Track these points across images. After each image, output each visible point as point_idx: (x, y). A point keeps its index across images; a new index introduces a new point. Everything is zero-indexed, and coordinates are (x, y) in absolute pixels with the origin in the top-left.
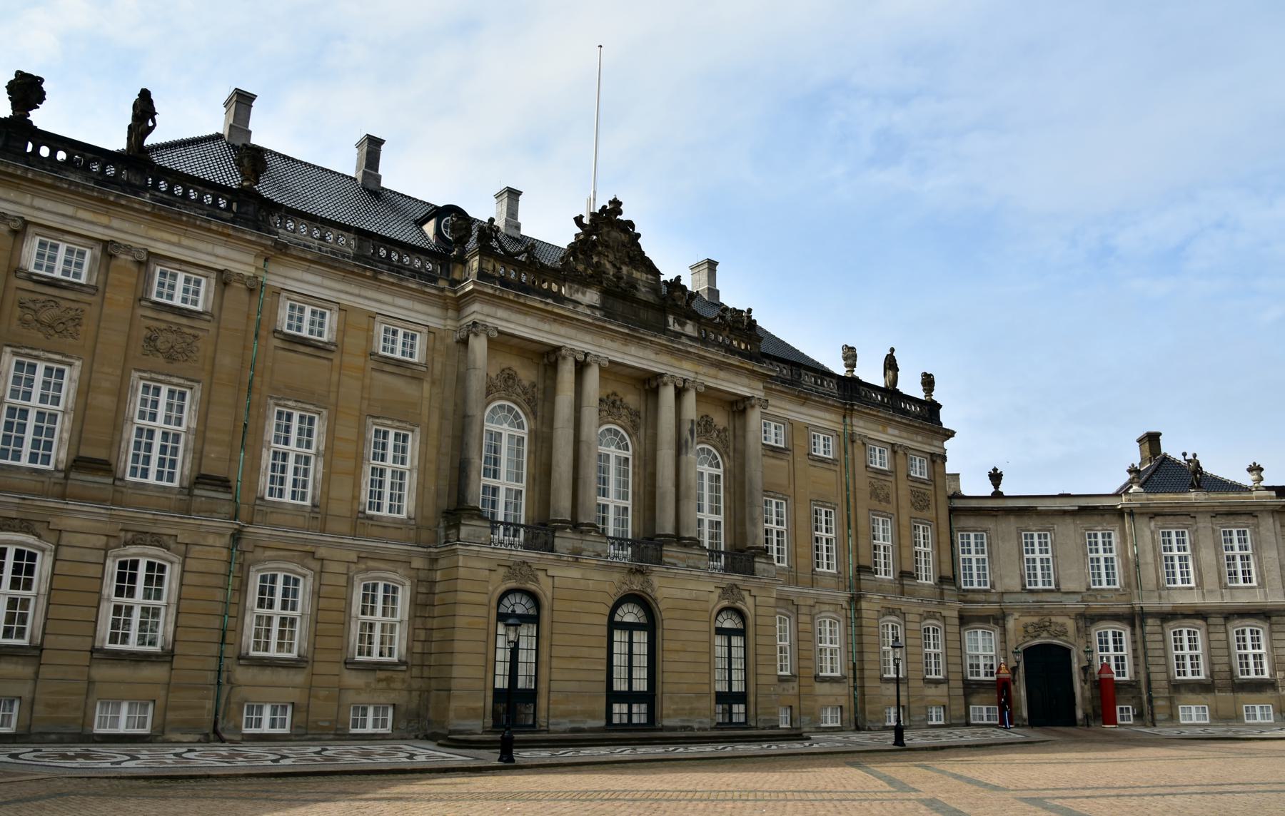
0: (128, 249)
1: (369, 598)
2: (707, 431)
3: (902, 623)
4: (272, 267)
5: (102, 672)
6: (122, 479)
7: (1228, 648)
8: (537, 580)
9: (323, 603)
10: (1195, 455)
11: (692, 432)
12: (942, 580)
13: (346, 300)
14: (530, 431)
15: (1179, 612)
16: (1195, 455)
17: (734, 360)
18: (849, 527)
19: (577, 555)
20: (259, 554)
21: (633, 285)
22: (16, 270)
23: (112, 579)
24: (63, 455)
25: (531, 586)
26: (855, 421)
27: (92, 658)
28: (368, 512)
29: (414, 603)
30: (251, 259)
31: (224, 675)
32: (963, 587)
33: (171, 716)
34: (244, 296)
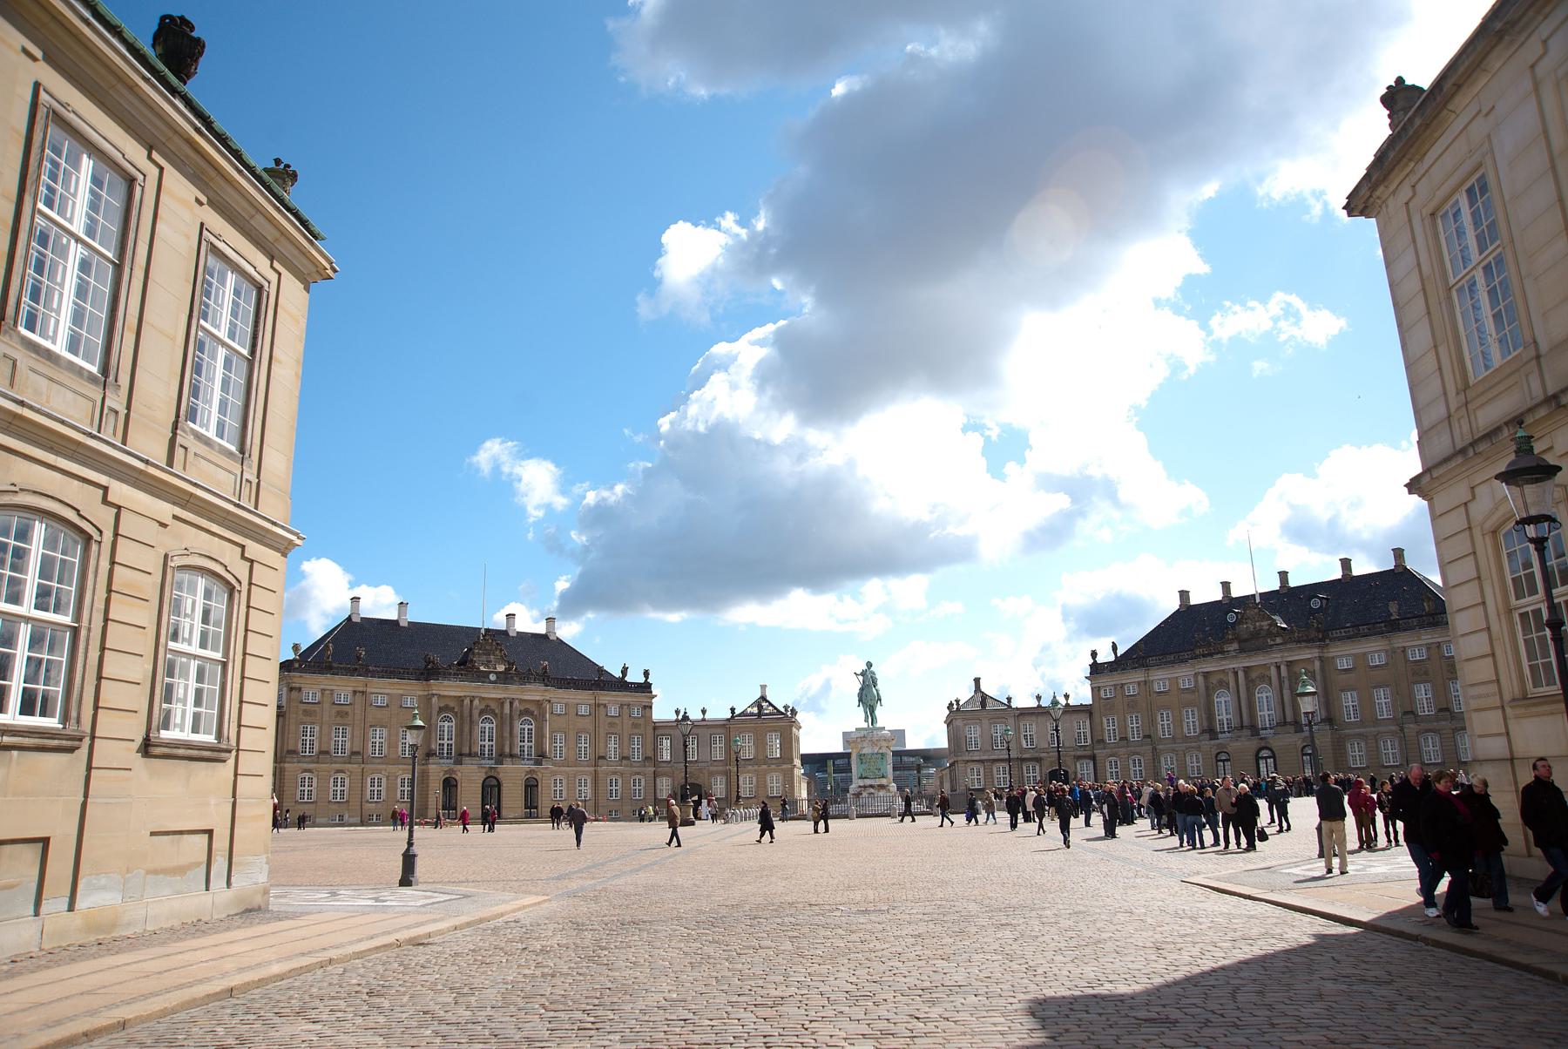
17: (1304, 644)
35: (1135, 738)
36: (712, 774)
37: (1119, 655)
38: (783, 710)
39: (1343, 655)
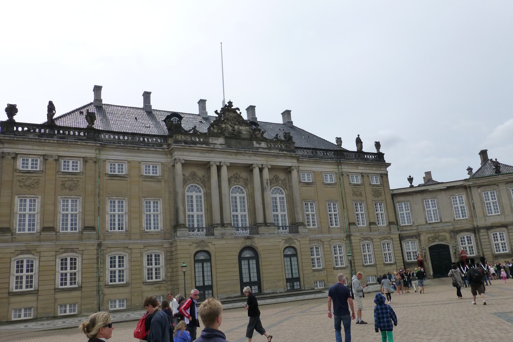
0: (51, 156)
1: (149, 260)
2: (276, 181)
3: (372, 243)
4: (102, 152)
5: (59, 295)
6: (59, 232)
8: (208, 246)
9: (133, 264)
10: (496, 159)
11: (267, 183)
12: (390, 223)
13: (130, 159)
14: (204, 193)
15: (494, 226)
16: (496, 159)
18: (344, 208)
19: (223, 236)
20: (108, 250)
21: (240, 132)
22: (16, 170)
23: (59, 265)
24: (39, 227)
25: (206, 249)
26: (343, 167)
27: (55, 292)
28: (146, 230)
29: (166, 260)
30: (93, 151)
31: (101, 292)
32: (401, 225)
33: (83, 307)
34: (93, 165)
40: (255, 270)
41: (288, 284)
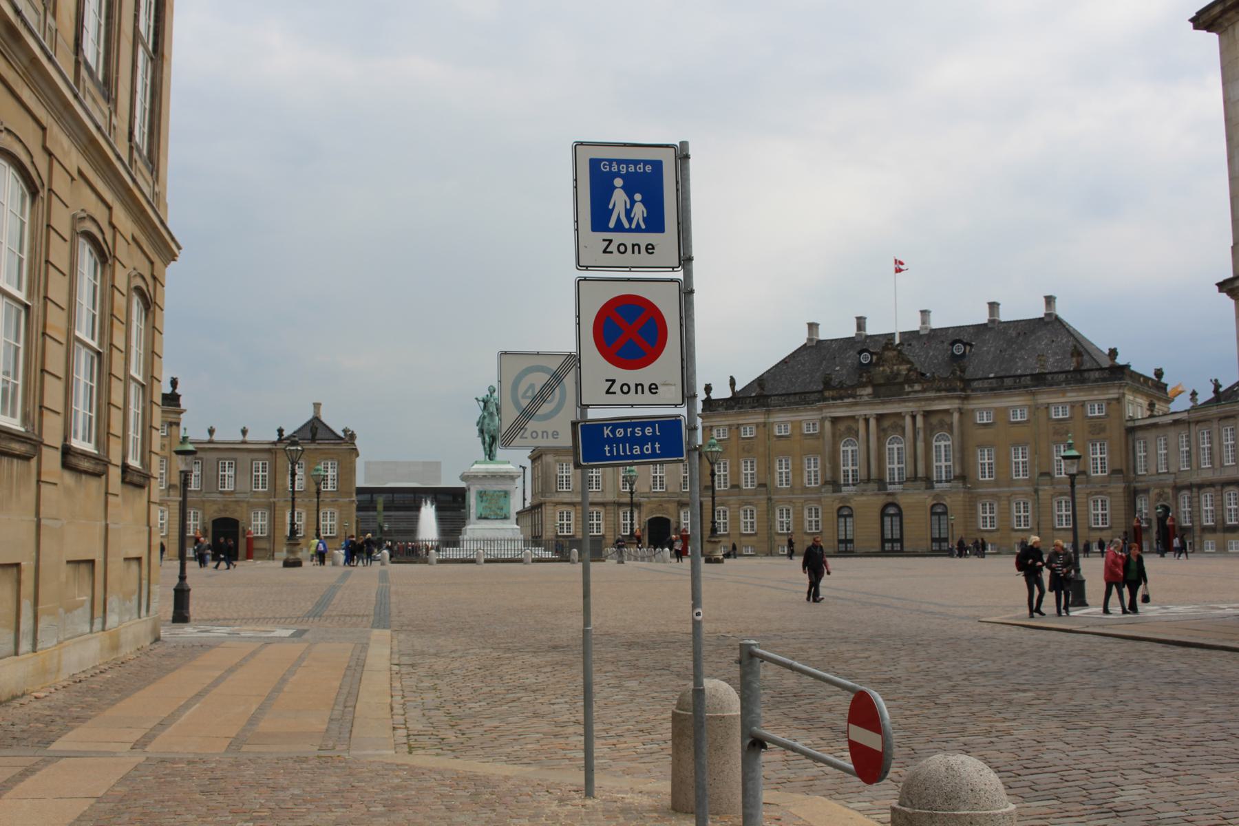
0: (733, 425)
7: (1222, 505)
8: (849, 502)
13: (793, 419)
16: (1216, 380)
17: (943, 394)
25: (848, 505)
26: (1039, 397)
35: (748, 486)
36: (252, 506)
37: (738, 388)
38: (342, 434)
39: (984, 409)
40: (898, 528)
41: (934, 544)
